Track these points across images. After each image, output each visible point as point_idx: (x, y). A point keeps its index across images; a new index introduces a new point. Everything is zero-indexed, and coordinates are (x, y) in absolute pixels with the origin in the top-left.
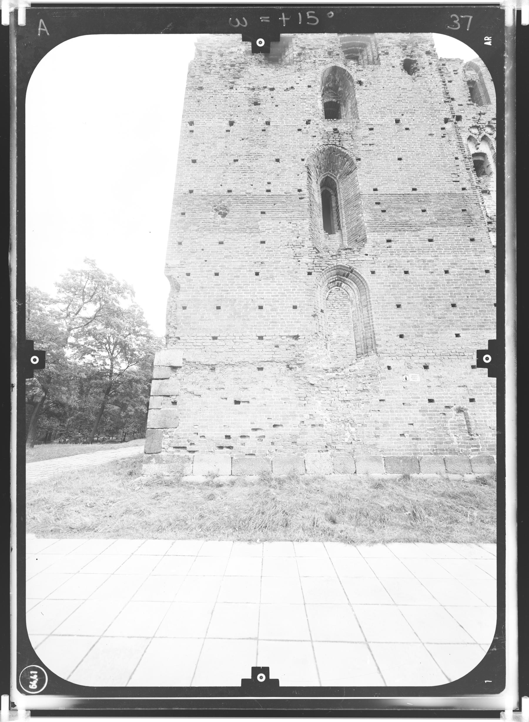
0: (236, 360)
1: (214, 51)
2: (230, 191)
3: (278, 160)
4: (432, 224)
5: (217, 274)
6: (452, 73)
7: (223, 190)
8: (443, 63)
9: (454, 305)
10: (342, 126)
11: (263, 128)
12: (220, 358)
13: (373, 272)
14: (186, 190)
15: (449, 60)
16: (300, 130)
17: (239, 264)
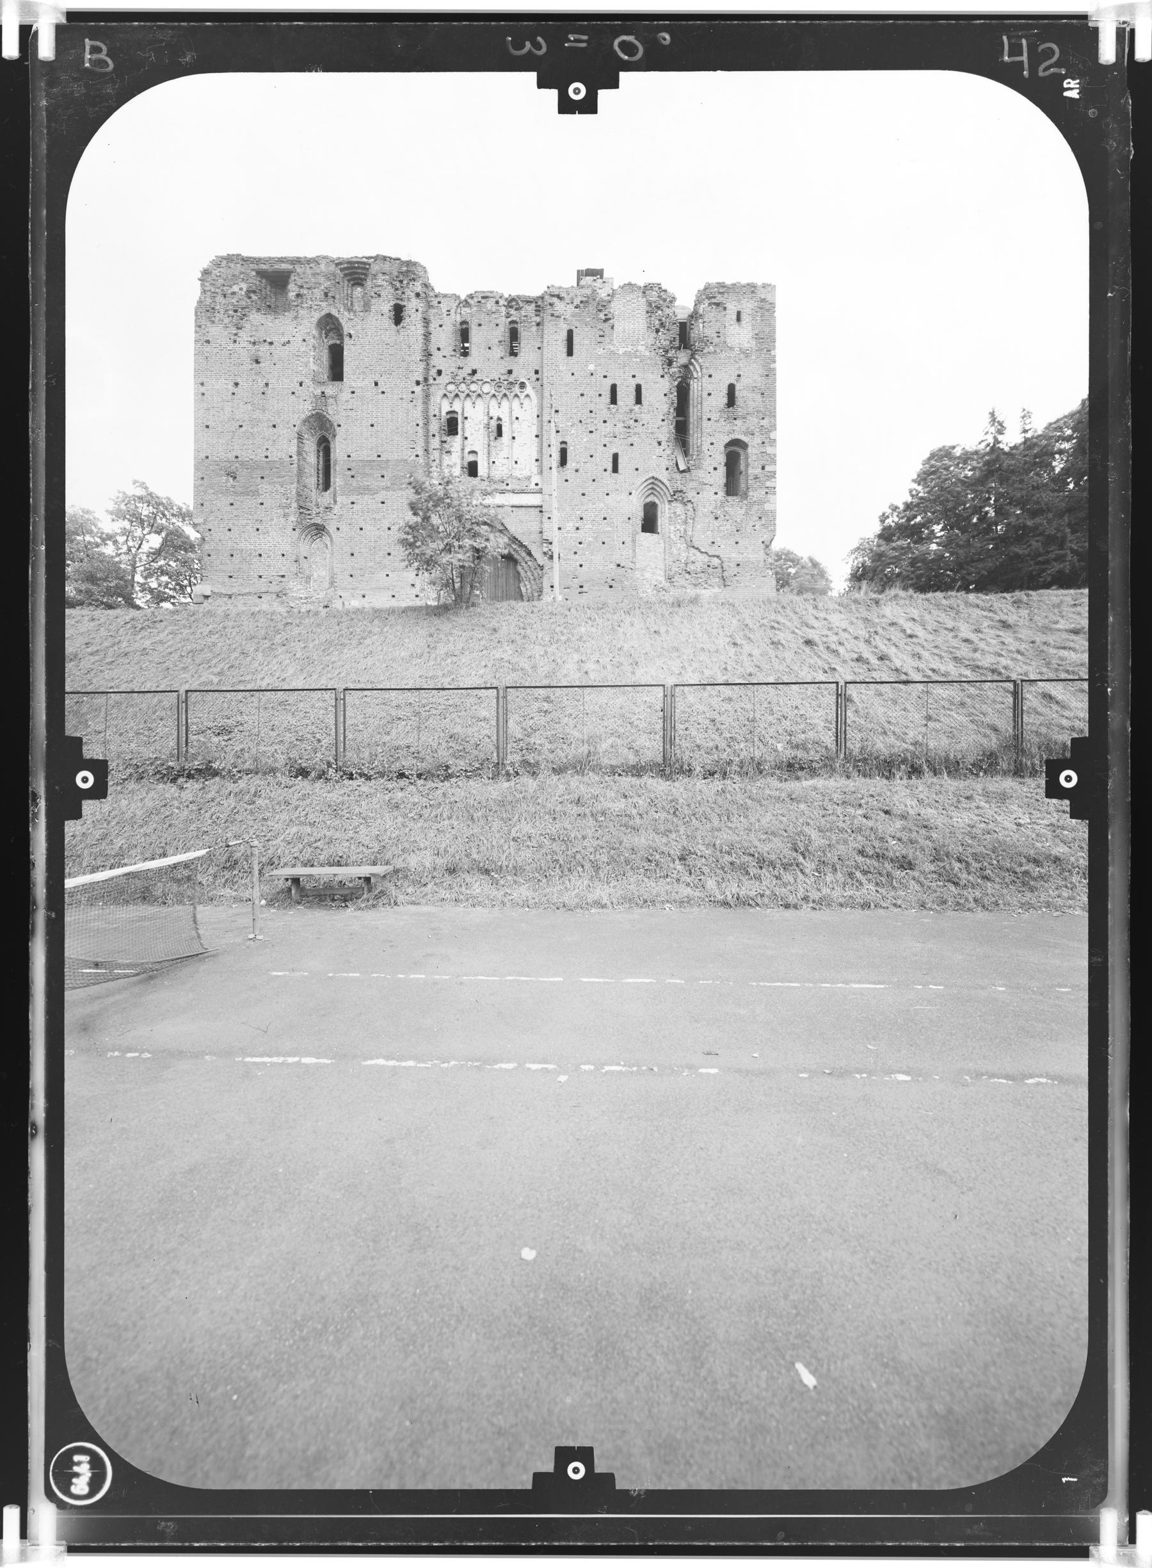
0: (245, 591)
1: (217, 290)
2: (237, 457)
3: (274, 426)
4: (387, 488)
5: (230, 530)
6: (445, 315)
7: (231, 456)
8: (439, 299)
9: (389, 554)
10: (331, 389)
11: (262, 390)
12: (234, 590)
13: (338, 529)
14: (203, 456)
15: (445, 296)
16: (293, 393)
17: (245, 521)
